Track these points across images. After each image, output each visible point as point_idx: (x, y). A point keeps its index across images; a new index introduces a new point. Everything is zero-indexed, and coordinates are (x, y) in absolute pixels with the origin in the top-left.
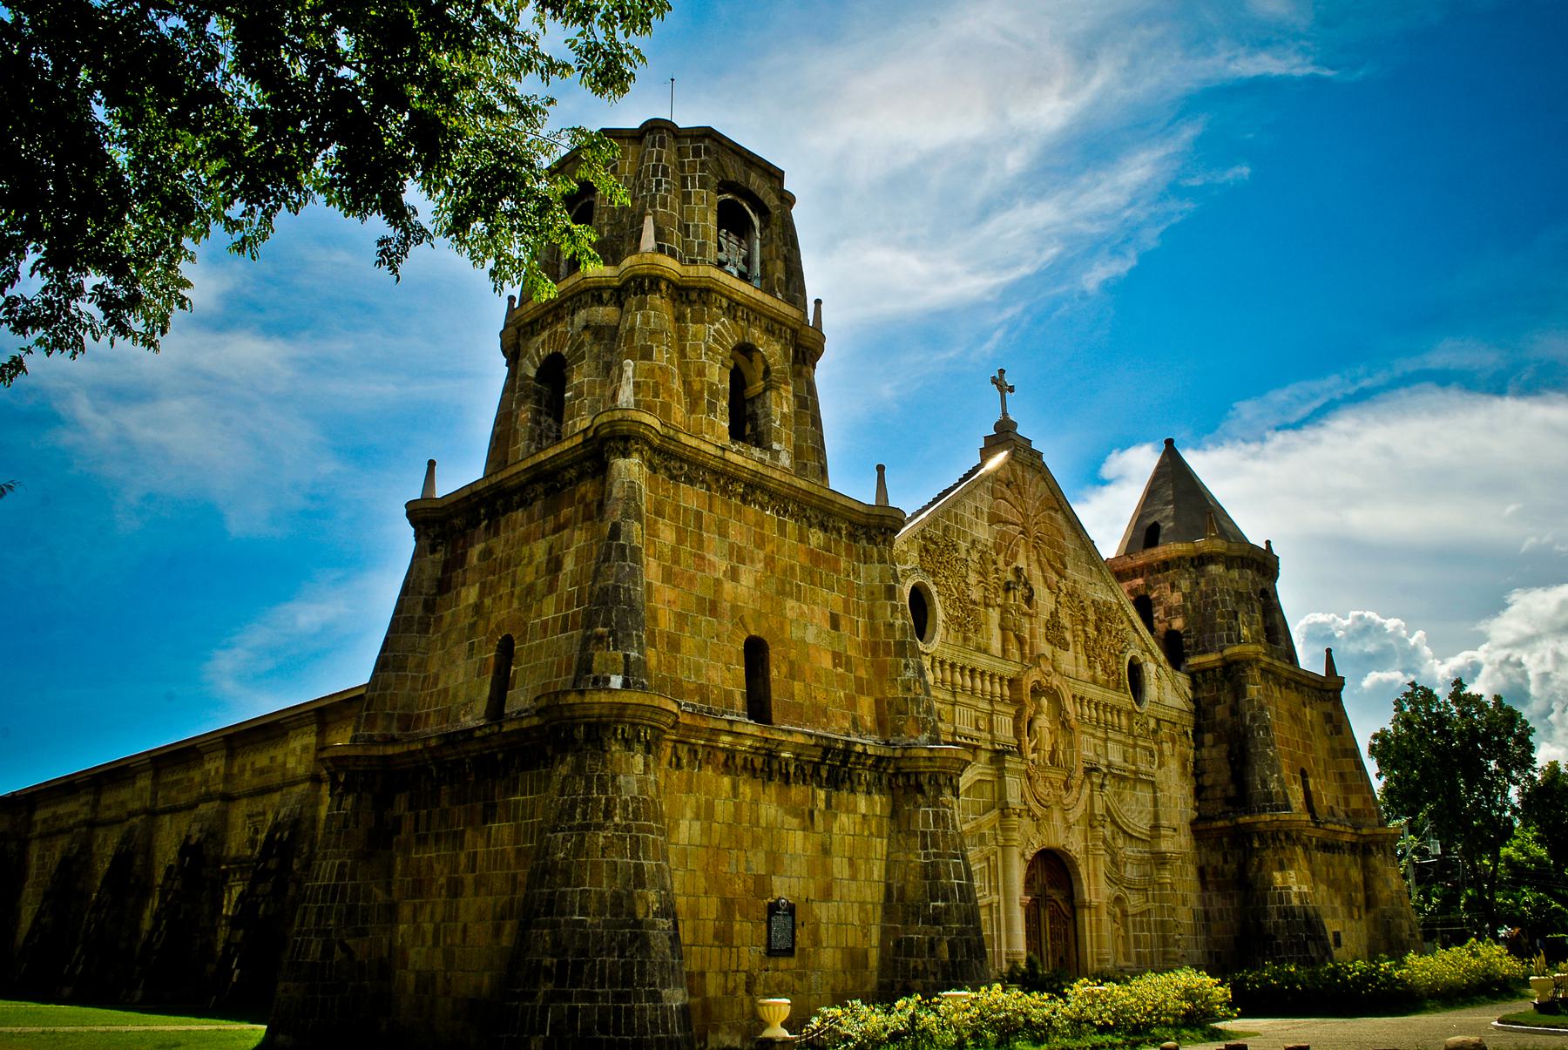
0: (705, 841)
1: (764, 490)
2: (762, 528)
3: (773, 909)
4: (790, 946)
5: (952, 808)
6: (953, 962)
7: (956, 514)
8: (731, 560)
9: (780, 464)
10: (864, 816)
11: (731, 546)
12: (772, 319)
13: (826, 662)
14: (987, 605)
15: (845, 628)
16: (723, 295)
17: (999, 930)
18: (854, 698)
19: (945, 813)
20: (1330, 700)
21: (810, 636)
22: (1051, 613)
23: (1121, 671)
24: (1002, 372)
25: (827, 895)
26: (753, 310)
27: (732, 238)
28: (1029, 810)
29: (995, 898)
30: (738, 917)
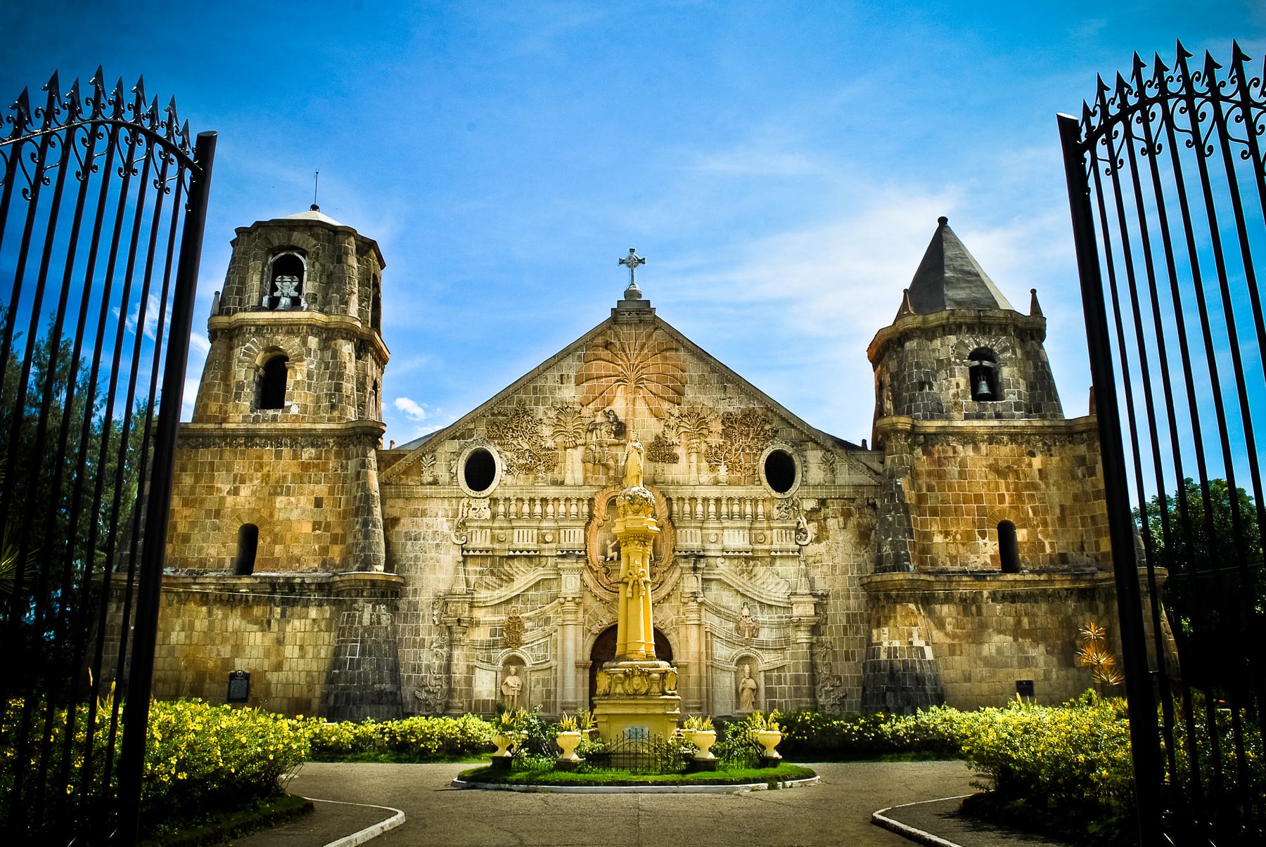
0: (188, 642)
1: (261, 437)
2: (262, 459)
3: (233, 676)
4: (244, 696)
5: (363, 611)
6: (334, 706)
7: (535, 388)
8: (234, 483)
9: (291, 413)
10: (314, 620)
11: (235, 476)
12: (291, 325)
13: (307, 528)
14: (565, 448)
15: (327, 506)
16: (251, 326)
17: (556, 686)
18: (328, 547)
19: (354, 614)
20: (1083, 441)
21: (295, 515)
22: (657, 437)
24: (632, 251)
25: (278, 667)
26: (275, 325)
27: (287, 278)
28: (596, 596)
29: (553, 663)
30: (208, 681)
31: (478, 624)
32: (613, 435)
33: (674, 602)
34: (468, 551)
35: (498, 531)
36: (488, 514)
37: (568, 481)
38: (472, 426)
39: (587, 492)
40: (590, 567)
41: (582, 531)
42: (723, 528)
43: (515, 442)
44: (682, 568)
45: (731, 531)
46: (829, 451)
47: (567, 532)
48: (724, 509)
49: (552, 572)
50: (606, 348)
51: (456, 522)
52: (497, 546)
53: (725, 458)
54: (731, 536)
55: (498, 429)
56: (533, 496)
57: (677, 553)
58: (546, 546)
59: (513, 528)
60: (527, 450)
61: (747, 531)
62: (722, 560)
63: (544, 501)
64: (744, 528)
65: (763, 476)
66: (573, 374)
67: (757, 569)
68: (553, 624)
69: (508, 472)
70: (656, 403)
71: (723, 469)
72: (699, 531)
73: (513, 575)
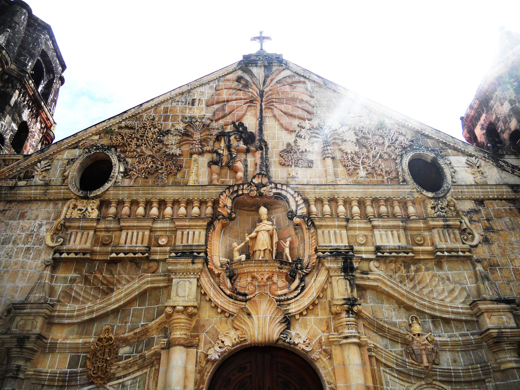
22: (289, 145)
23: (400, 170)
28: (216, 307)
31: (53, 348)
32: (241, 142)
33: (322, 314)
34: (61, 254)
35: (103, 234)
36: (95, 214)
37: (191, 183)
38: (97, 137)
39: (213, 192)
40: (211, 271)
41: (203, 233)
42: (374, 227)
43: (139, 150)
44: (328, 269)
45: (383, 232)
46: (471, 156)
47: (185, 232)
48: (370, 210)
49: (161, 278)
50: (237, 81)
51: (56, 222)
52: (98, 248)
53: (363, 163)
54: (384, 237)
55: (123, 139)
56: (149, 197)
57: (320, 254)
58: (158, 249)
59: (121, 229)
60: (150, 156)
61: (401, 232)
62: (377, 264)
63: (162, 204)
64: (397, 227)
65: (408, 178)
66: (205, 98)
67: (421, 274)
68: (156, 347)
69: (126, 174)
70: (286, 120)
71: (362, 173)
72: (344, 232)
73: (113, 284)
